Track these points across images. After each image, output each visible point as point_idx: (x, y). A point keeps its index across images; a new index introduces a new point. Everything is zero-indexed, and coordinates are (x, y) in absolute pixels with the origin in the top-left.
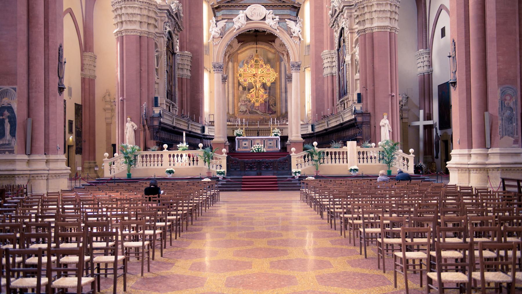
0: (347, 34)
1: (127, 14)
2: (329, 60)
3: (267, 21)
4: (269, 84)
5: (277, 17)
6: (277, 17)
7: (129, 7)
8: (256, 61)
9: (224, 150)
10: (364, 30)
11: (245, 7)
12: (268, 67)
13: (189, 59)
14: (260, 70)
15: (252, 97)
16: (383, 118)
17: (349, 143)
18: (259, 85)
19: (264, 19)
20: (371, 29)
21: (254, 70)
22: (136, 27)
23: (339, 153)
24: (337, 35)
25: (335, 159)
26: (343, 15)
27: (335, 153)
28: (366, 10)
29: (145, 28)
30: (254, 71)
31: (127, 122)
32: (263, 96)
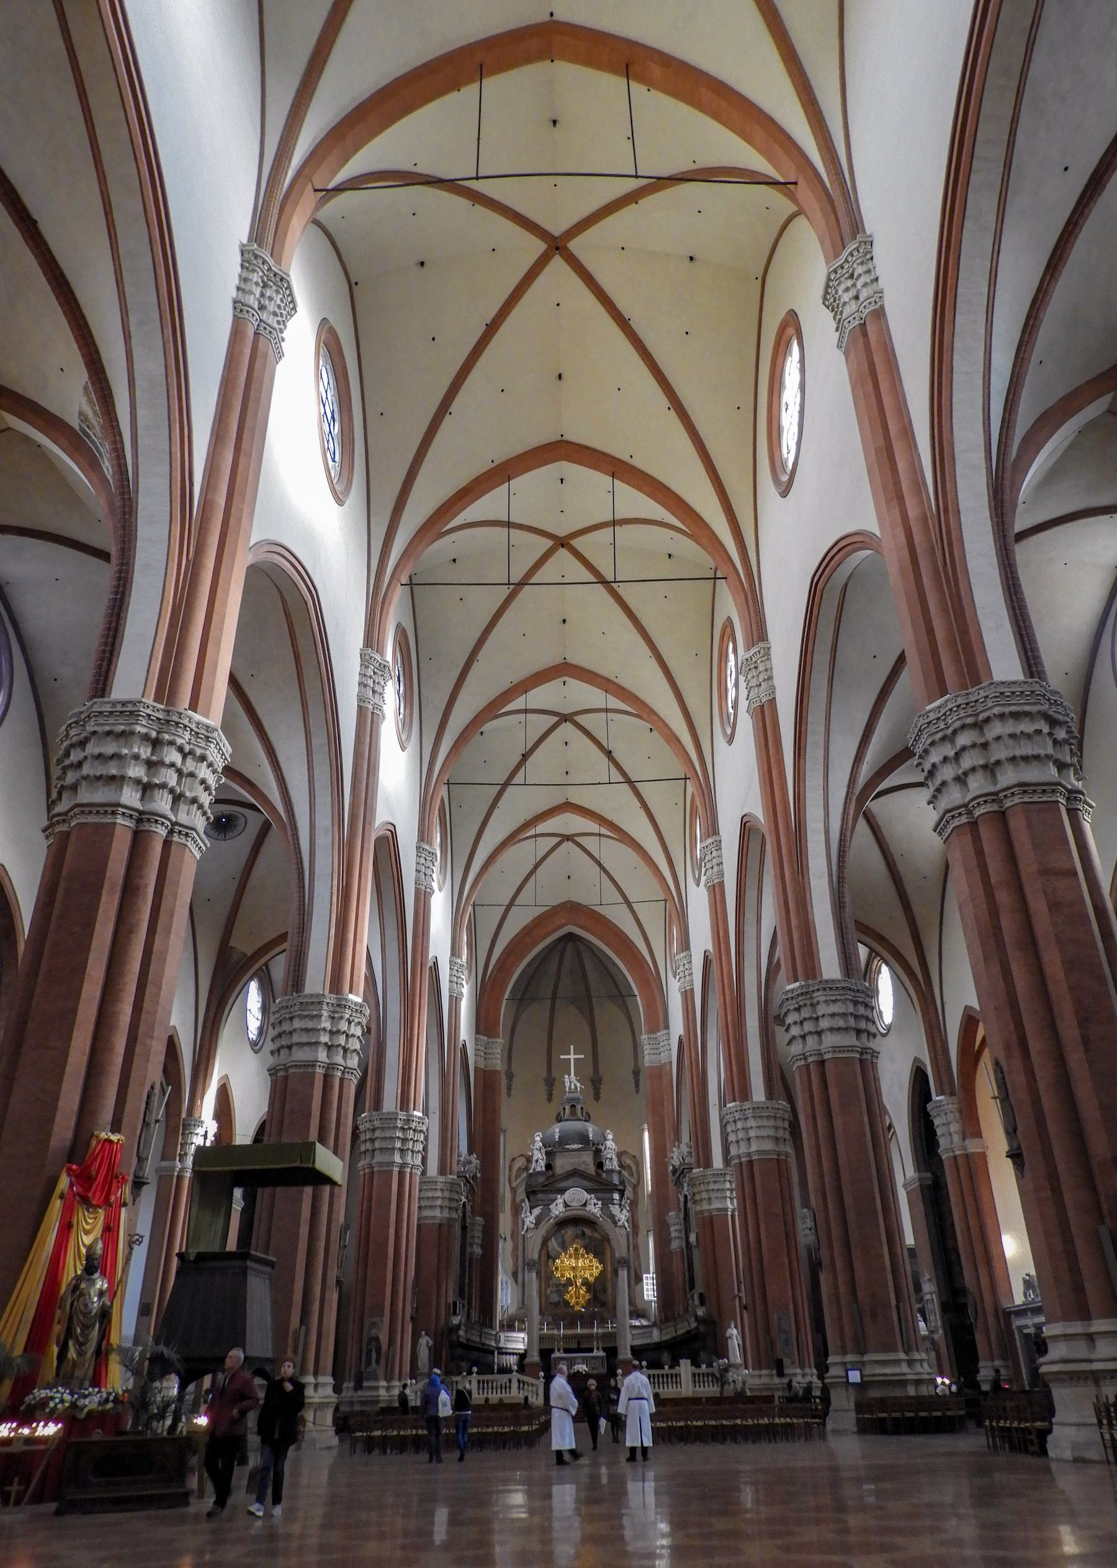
0: (689, 1204)
1: (428, 1198)
2: (677, 1227)
3: (587, 1208)
4: (591, 1279)
5: (600, 1202)
6: (600, 1202)
7: (432, 1189)
8: (576, 1250)
9: (542, 1374)
10: (702, 1212)
11: (562, 1191)
12: (591, 1256)
13: (480, 1228)
14: (580, 1261)
15: (571, 1297)
16: (729, 1327)
17: (683, 1362)
18: (579, 1281)
19: (585, 1205)
20: (709, 1211)
21: (573, 1261)
22: (437, 1213)
23: (699, 1375)
24: (682, 1199)
25: (663, 1383)
26: (685, 1177)
27: (658, 1375)
28: (702, 1187)
29: (446, 1214)
30: (573, 1262)
31: (420, 1336)
32: (584, 1297)
